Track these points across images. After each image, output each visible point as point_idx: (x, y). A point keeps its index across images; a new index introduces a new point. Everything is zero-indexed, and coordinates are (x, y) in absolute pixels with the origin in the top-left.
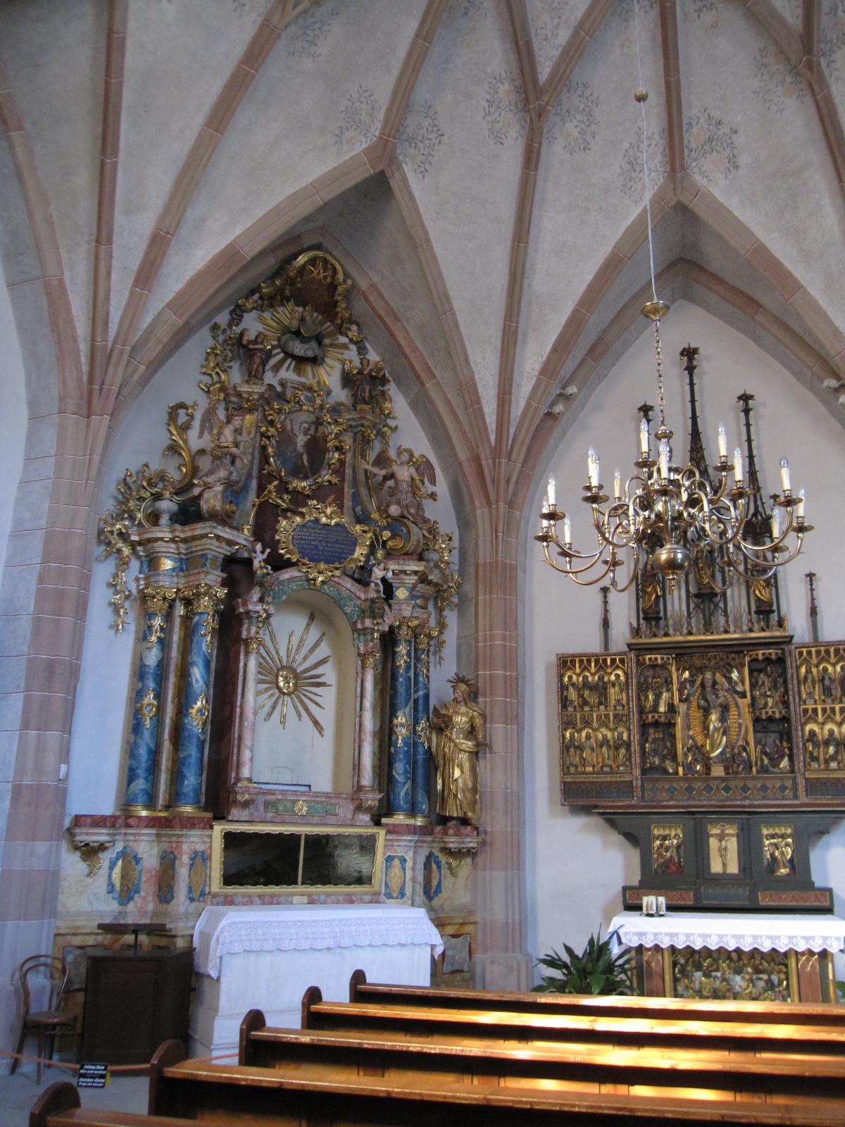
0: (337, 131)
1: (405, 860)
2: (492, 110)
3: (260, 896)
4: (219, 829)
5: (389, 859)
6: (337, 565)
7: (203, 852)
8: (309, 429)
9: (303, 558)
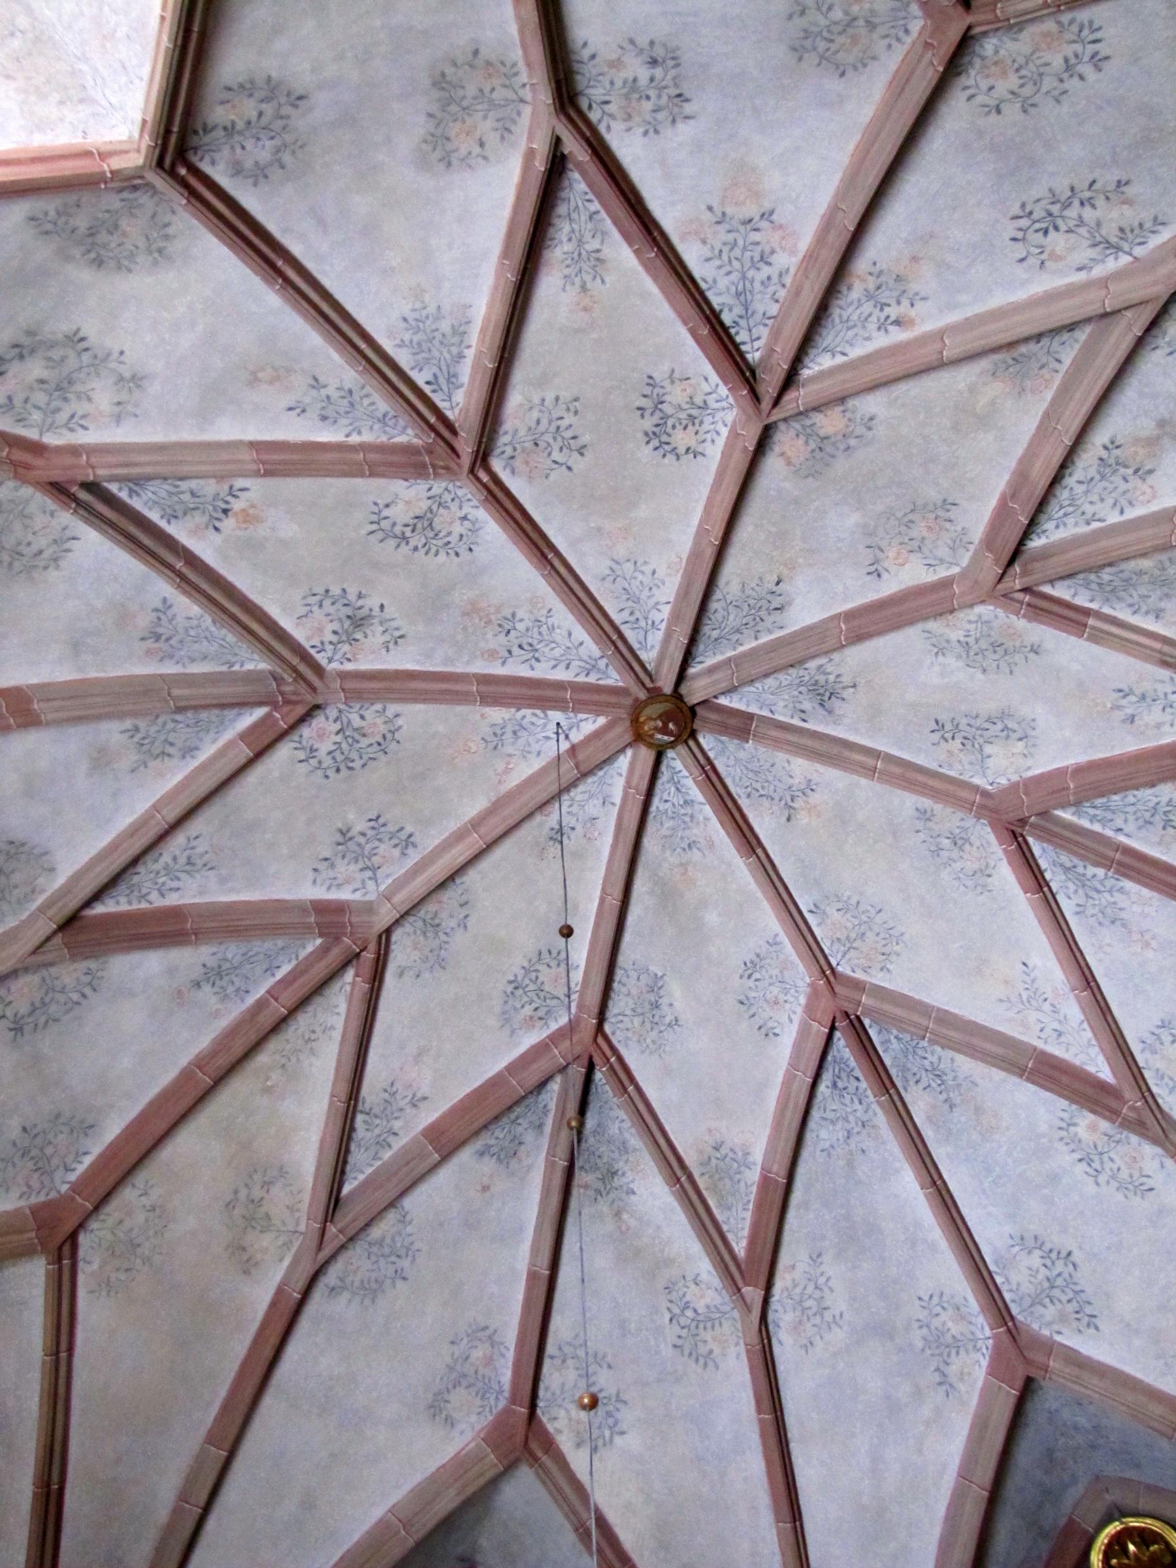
0: (937, 1378)
2: (1096, 1165)
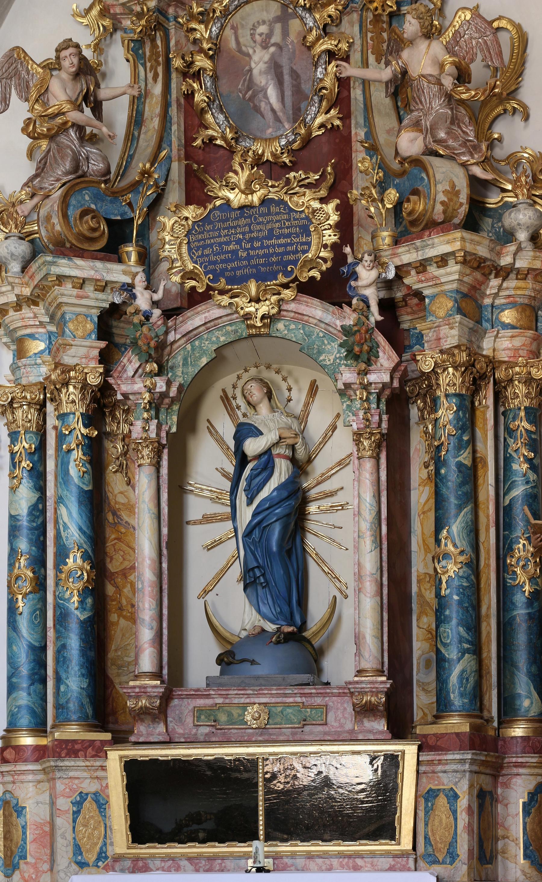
1: (456, 796)
3: (190, 859)
4: (115, 759)
6: (281, 279)
7: (96, 794)
8: (269, 35)
9: (215, 280)
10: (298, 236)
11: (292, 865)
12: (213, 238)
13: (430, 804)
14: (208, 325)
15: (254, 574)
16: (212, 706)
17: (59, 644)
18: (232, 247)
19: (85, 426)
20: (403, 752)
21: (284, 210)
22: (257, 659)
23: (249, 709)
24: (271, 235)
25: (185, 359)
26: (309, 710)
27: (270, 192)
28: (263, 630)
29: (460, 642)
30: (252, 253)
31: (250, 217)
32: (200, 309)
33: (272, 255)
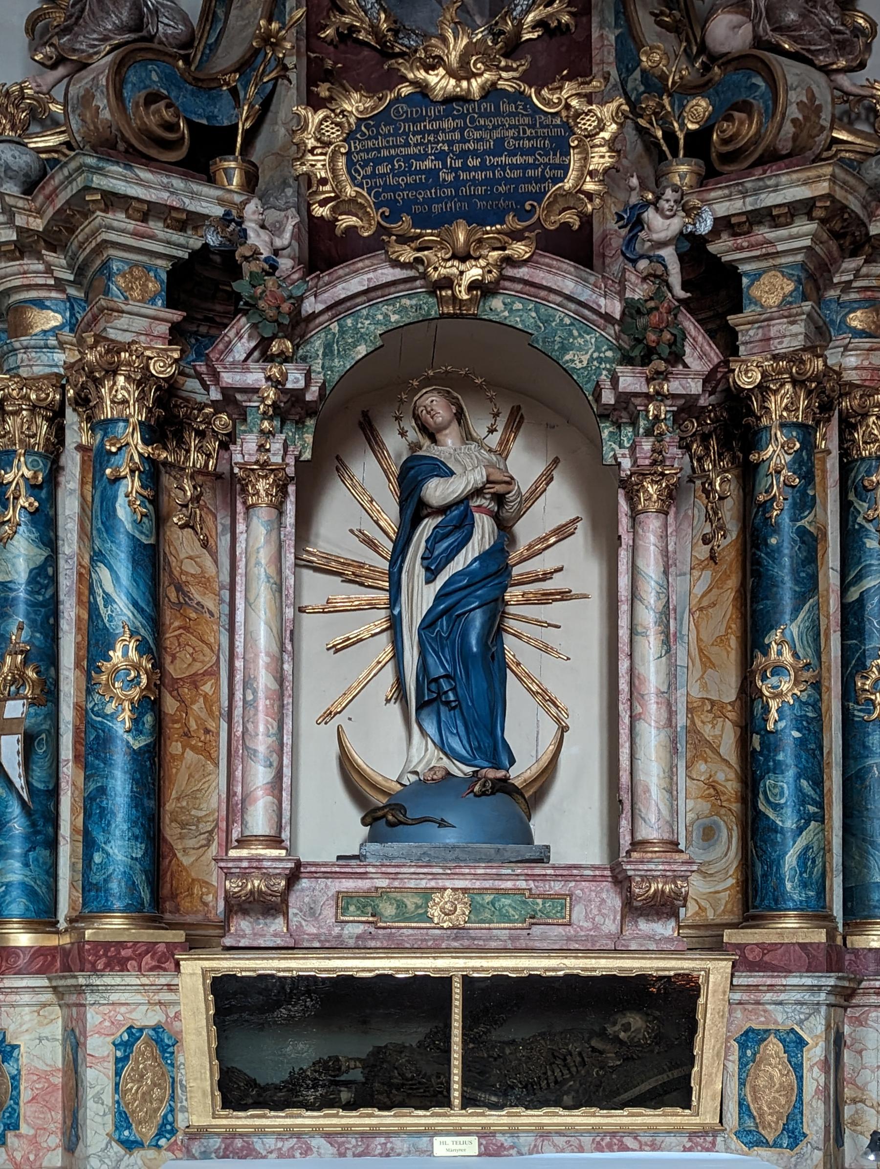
1: (801, 1043)
5: (750, 1040)
9: (394, 217)
10: (547, 154)
11: (512, 1147)
12: (394, 147)
13: (749, 1053)
14: (373, 294)
15: (439, 687)
16: (369, 891)
17: (92, 786)
18: (428, 164)
19: (146, 442)
20: (708, 973)
21: (525, 109)
22: (450, 820)
23: (437, 897)
24: (499, 148)
25: (328, 347)
26: (540, 901)
27: (501, 78)
28: (448, 773)
29: (803, 803)
30: (463, 176)
31: (463, 116)
32: (360, 265)
33: (499, 182)
